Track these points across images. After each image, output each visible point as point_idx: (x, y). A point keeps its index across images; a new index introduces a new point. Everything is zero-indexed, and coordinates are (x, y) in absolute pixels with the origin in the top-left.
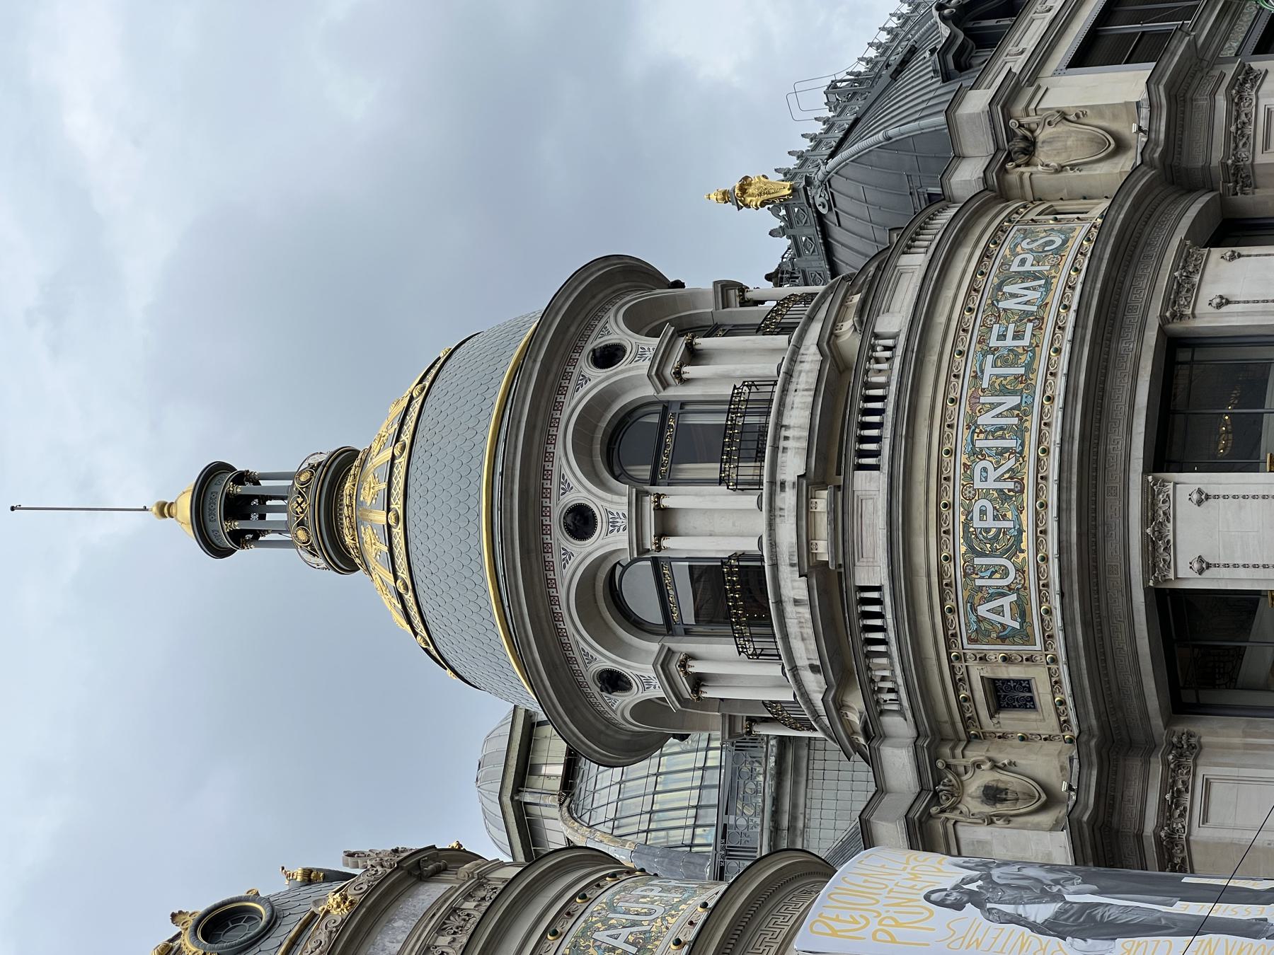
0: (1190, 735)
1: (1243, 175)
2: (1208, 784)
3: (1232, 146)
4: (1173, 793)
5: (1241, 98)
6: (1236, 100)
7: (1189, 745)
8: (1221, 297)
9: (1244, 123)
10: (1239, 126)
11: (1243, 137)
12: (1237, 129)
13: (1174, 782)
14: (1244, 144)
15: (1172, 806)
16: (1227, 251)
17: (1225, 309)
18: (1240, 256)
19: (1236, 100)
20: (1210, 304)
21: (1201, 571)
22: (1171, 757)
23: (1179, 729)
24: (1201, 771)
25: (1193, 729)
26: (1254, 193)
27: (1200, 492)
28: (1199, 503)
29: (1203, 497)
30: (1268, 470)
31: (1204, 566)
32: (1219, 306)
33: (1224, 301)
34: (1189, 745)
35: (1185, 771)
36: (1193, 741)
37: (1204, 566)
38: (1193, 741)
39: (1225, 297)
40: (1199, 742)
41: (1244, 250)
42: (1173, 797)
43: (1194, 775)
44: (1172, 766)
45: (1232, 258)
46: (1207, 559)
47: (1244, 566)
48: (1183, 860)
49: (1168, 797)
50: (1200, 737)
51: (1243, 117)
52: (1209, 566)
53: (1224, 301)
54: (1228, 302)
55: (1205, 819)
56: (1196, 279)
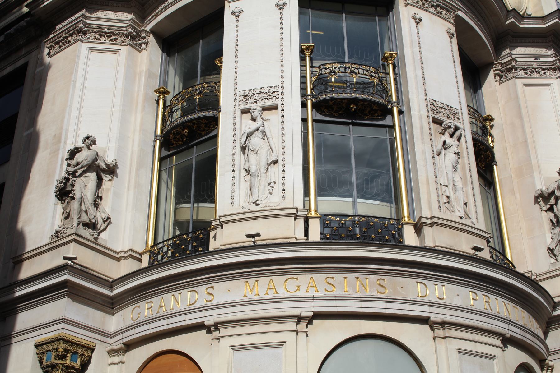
0: (147, 44)
1: (506, 75)
2: (116, 51)
3: (524, 67)
4: (109, 33)
5: (555, 70)
6: (553, 67)
7: (141, 45)
8: (420, 20)
9: (539, 73)
10: (537, 70)
11: (531, 72)
12: (535, 69)
13: (117, 35)
14: (526, 73)
15: (101, 33)
16: (453, 30)
17: (413, 21)
18: (451, 38)
19: (553, 67)
20: (415, 13)
21: (234, 13)
22: (130, 30)
23: (151, 39)
24: (124, 50)
25: (150, 45)
26: (496, 81)
27: (285, 4)
28: (277, 5)
29: (281, 7)
30: (302, 44)
31: (236, 15)
32: (414, 18)
33: (418, 21)
34: (141, 45)
35: (123, 40)
36: (144, 46)
37: (237, 14)
38: (144, 46)
39: (421, 23)
40: (143, 49)
41: (455, 40)
42: (106, 33)
43: (121, 45)
44: (126, 32)
45: (448, 33)
46: (242, 15)
47: (237, 35)
48: (69, 42)
49: (106, 30)
50: (146, 50)
51: (542, 72)
52: (237, 17)
53: (418, 21)
54: (418, 23)
55: (92, 50)
56: (432, 10)
